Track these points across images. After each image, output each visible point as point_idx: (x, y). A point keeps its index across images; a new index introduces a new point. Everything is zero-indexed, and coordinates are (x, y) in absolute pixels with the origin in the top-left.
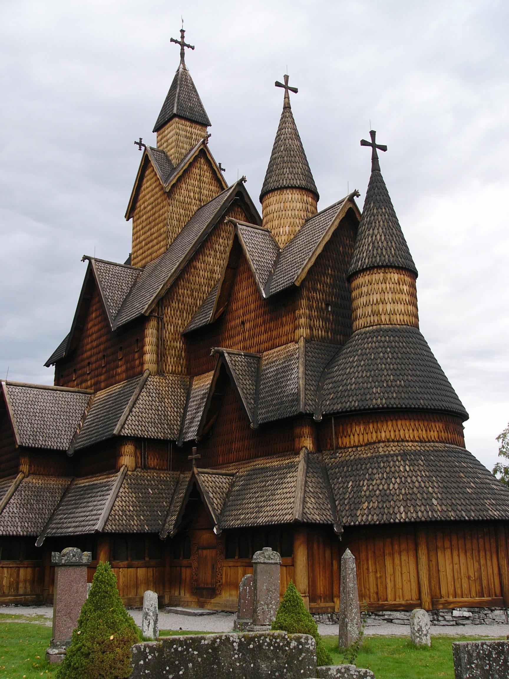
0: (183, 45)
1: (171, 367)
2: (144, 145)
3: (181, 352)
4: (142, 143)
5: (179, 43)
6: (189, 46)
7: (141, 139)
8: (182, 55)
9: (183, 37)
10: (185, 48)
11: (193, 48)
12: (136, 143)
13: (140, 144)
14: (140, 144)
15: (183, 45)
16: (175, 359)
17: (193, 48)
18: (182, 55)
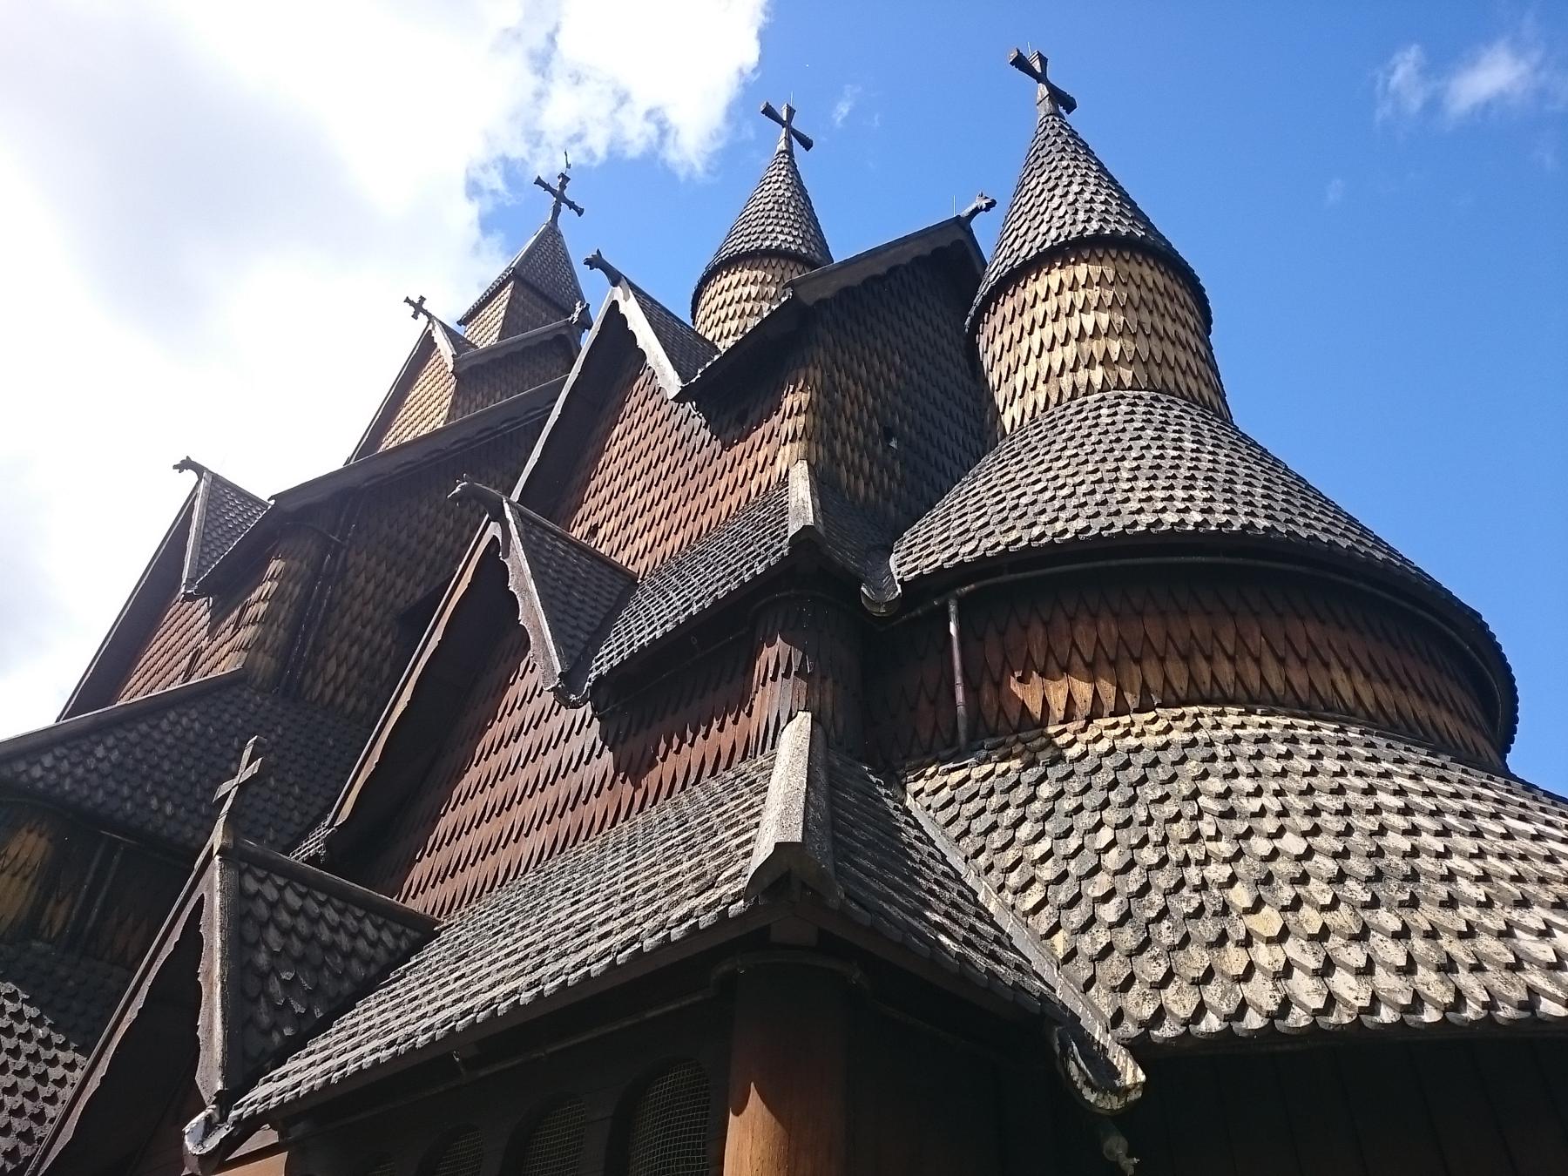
0: (560, 197)
1: (329, 691)
2: (426, 313)
3: (384, 660)
4: (425, 306)
5: (553, 192)
6: (571, 205)
7: (422, 299)
8: (556, 211)
9: (563, 186)
10: (564, 206)
11: (580, 212)
12: (407, 300)
13: (418, 307)
14: (418, 307)
15: (560, 197)
16: (355, 673)
17: (580, 212)
18: (556, 211)
